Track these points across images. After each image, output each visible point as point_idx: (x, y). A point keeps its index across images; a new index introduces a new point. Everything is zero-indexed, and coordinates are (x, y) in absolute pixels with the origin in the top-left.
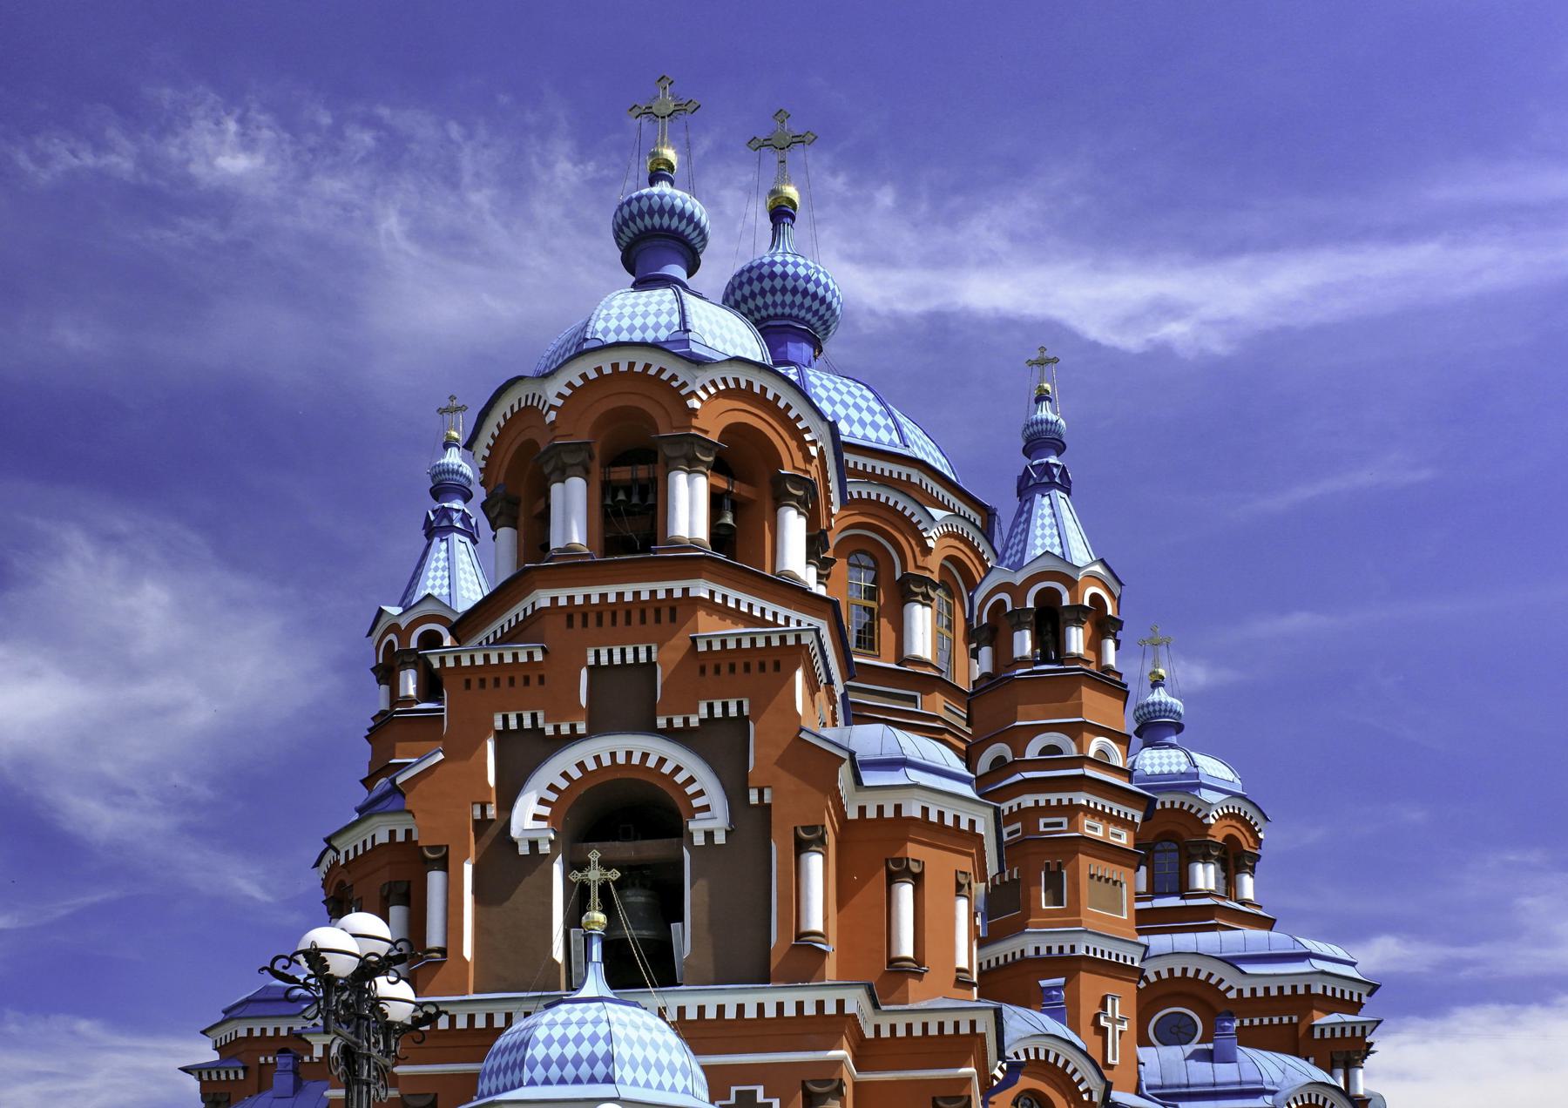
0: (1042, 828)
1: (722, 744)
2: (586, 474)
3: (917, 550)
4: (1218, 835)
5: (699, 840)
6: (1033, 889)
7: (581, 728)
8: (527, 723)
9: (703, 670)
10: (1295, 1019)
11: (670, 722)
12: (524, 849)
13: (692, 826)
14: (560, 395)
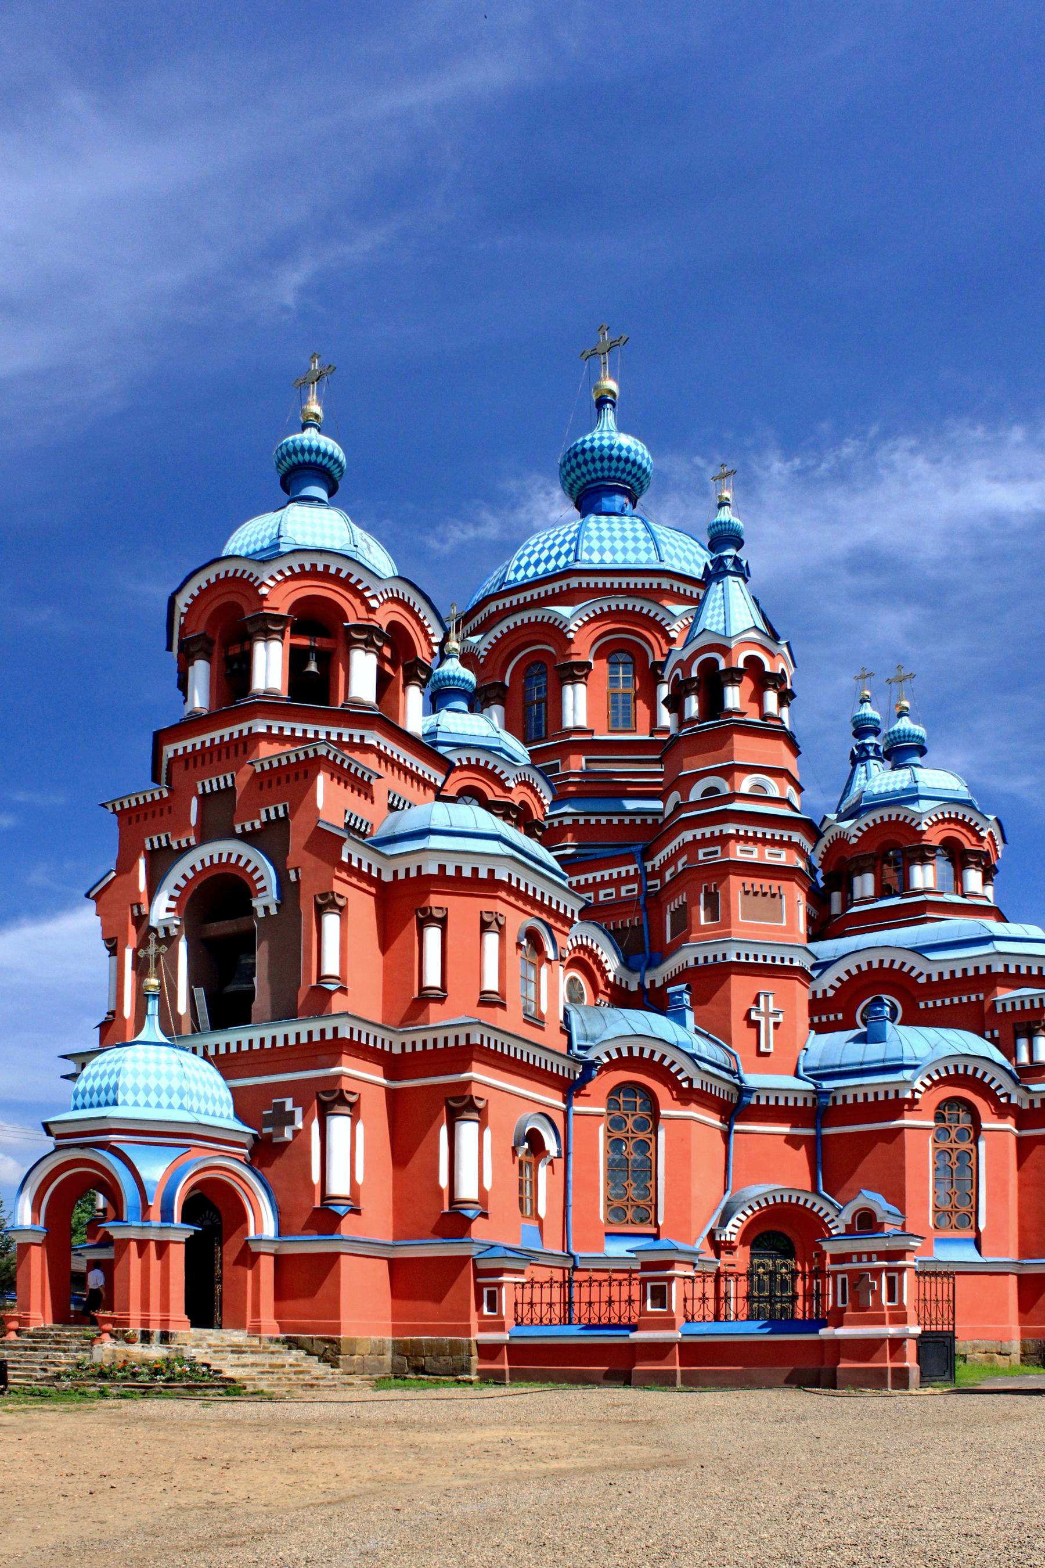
0: (701, 857)
2: (208, 657)
3: (663, 642)
4: (933, 838)
5: (261, 914)
6: (694, 909)
10: (982, 997)
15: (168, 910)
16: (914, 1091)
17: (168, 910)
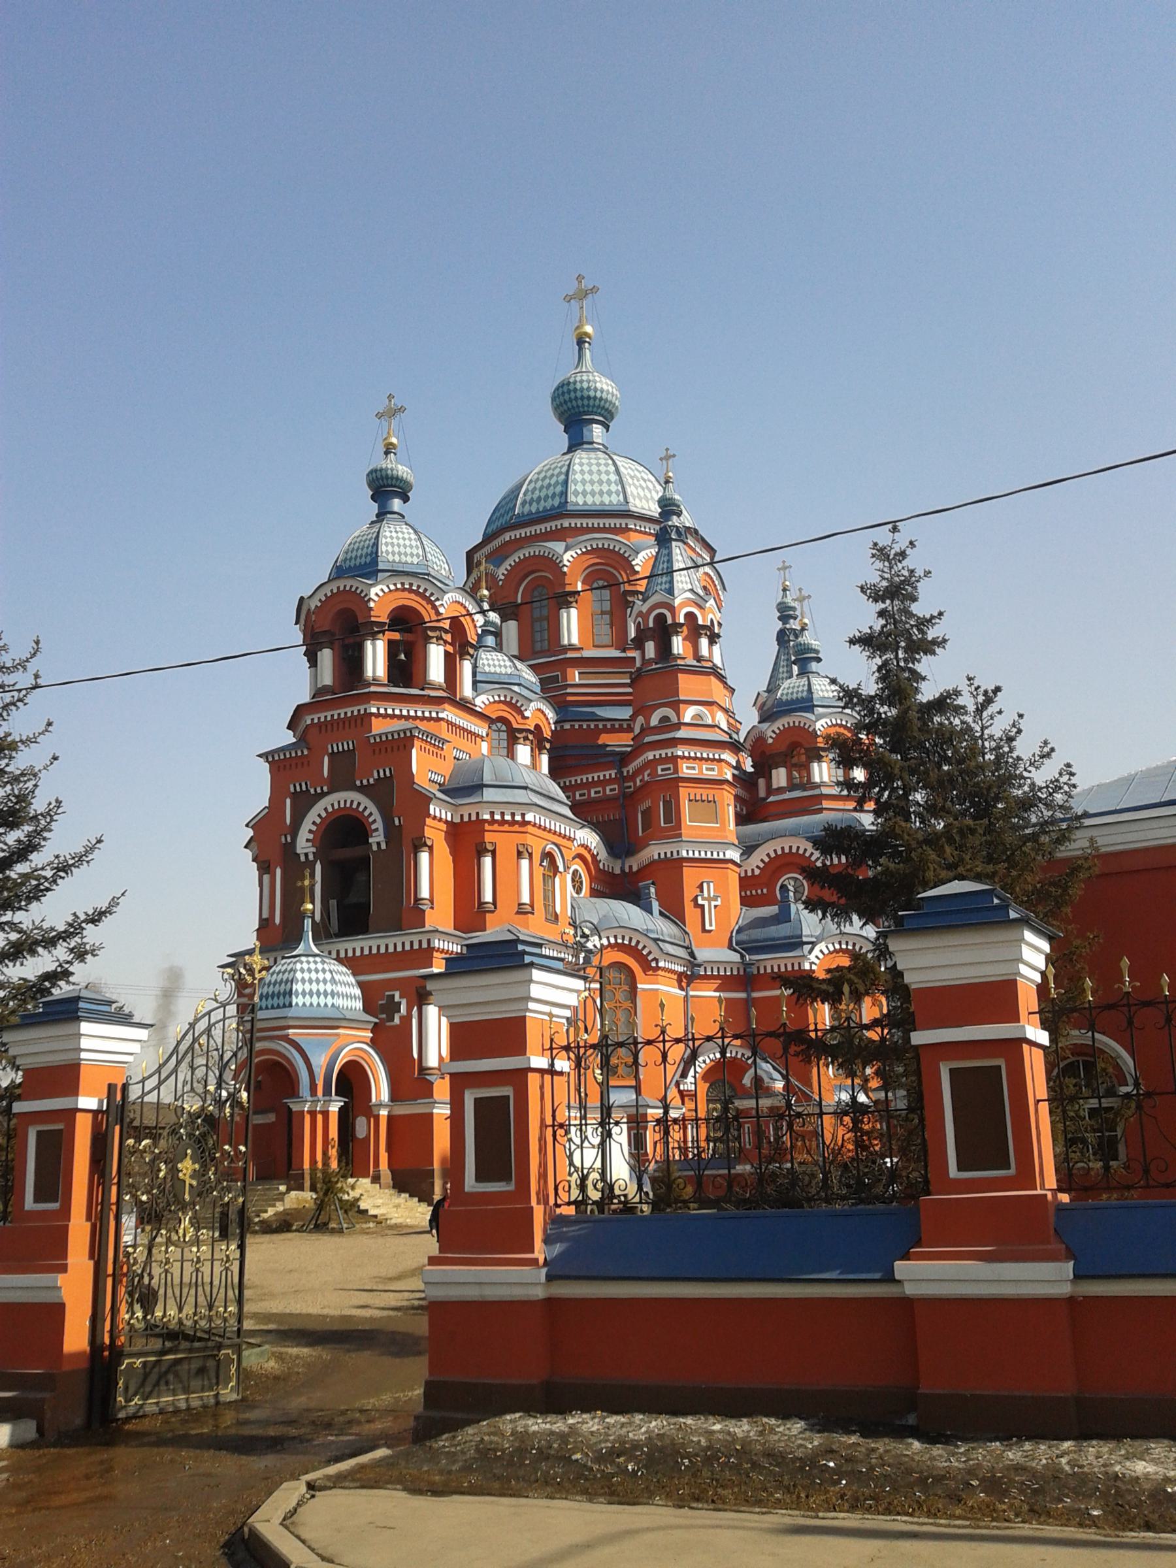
0: (660, 772)
5: (375, 848)
7: (325, 789)
16: (812, 963)
17: (308, 840)
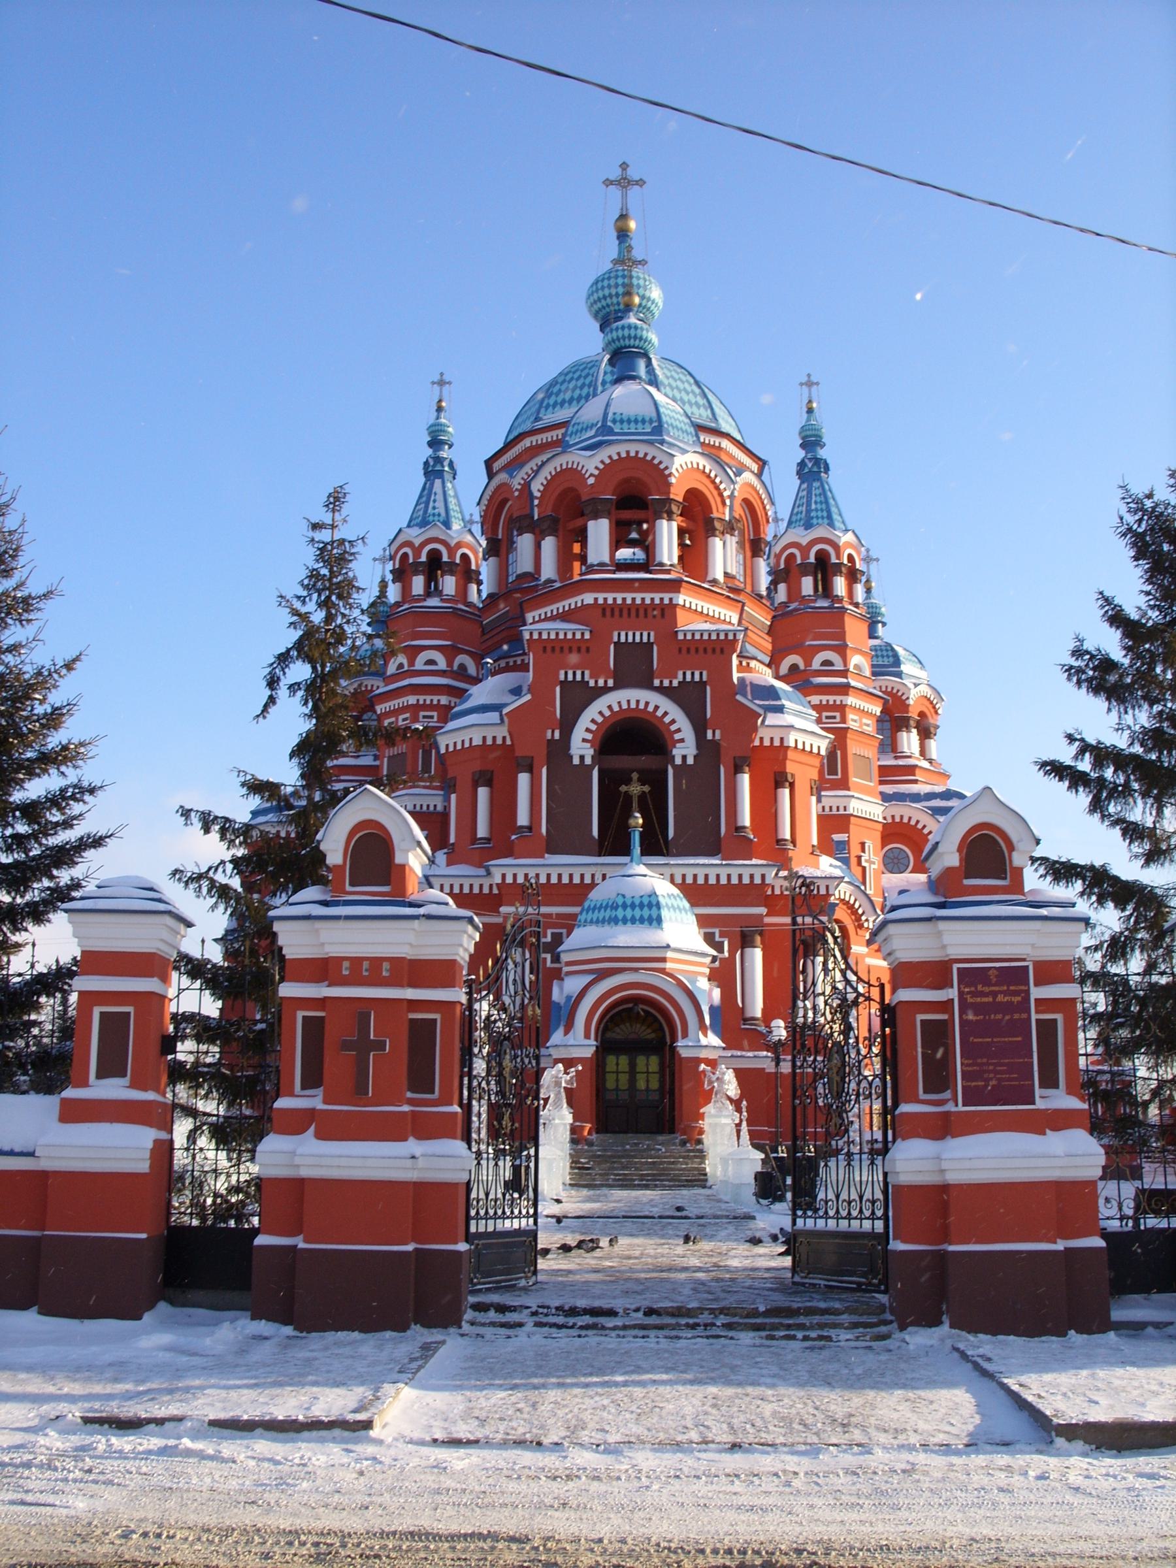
1: (688, 697)
5: (678, 761)
8: (579, 678)
9: (680, 650)
11: (661, 682)
12: (576, 761)
13: (675, 752)
14: (597, 468)
15: (584, 740)
